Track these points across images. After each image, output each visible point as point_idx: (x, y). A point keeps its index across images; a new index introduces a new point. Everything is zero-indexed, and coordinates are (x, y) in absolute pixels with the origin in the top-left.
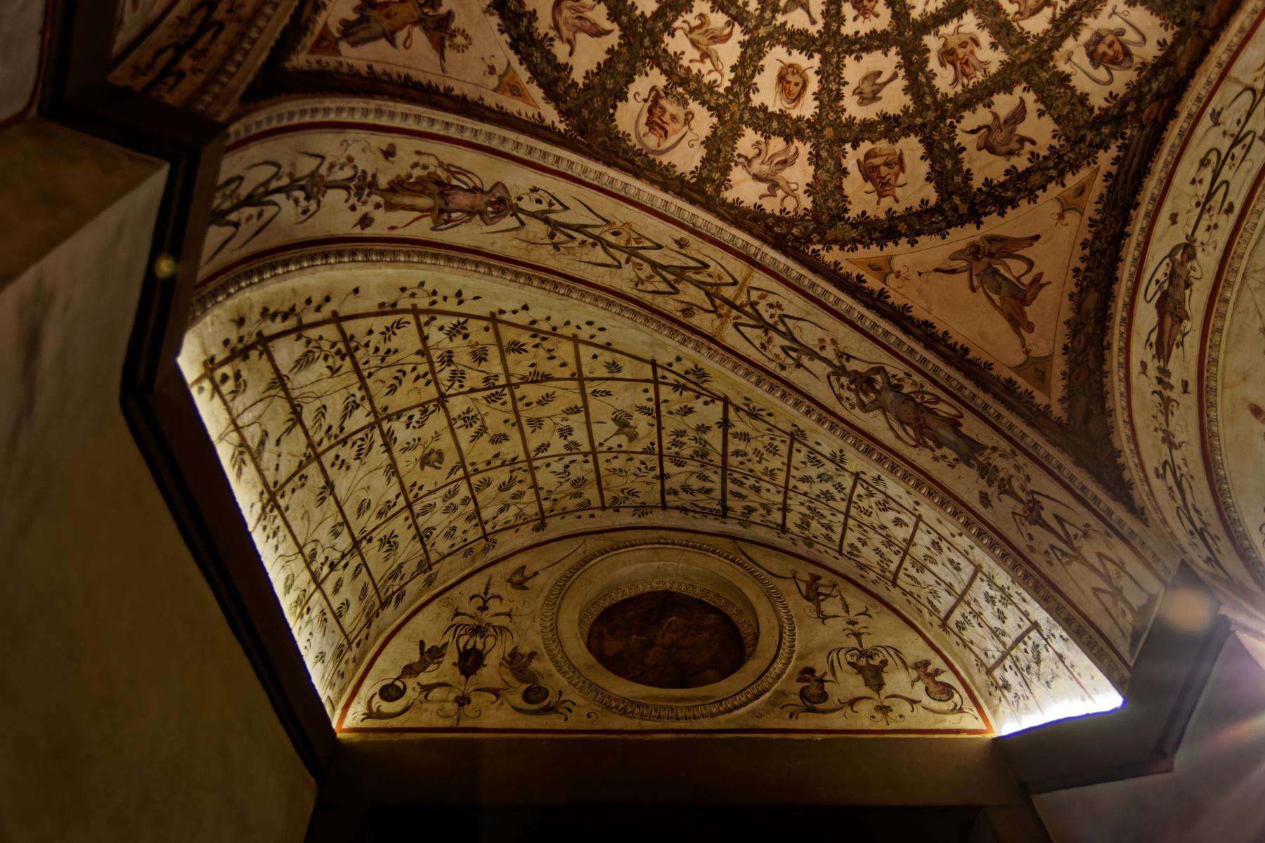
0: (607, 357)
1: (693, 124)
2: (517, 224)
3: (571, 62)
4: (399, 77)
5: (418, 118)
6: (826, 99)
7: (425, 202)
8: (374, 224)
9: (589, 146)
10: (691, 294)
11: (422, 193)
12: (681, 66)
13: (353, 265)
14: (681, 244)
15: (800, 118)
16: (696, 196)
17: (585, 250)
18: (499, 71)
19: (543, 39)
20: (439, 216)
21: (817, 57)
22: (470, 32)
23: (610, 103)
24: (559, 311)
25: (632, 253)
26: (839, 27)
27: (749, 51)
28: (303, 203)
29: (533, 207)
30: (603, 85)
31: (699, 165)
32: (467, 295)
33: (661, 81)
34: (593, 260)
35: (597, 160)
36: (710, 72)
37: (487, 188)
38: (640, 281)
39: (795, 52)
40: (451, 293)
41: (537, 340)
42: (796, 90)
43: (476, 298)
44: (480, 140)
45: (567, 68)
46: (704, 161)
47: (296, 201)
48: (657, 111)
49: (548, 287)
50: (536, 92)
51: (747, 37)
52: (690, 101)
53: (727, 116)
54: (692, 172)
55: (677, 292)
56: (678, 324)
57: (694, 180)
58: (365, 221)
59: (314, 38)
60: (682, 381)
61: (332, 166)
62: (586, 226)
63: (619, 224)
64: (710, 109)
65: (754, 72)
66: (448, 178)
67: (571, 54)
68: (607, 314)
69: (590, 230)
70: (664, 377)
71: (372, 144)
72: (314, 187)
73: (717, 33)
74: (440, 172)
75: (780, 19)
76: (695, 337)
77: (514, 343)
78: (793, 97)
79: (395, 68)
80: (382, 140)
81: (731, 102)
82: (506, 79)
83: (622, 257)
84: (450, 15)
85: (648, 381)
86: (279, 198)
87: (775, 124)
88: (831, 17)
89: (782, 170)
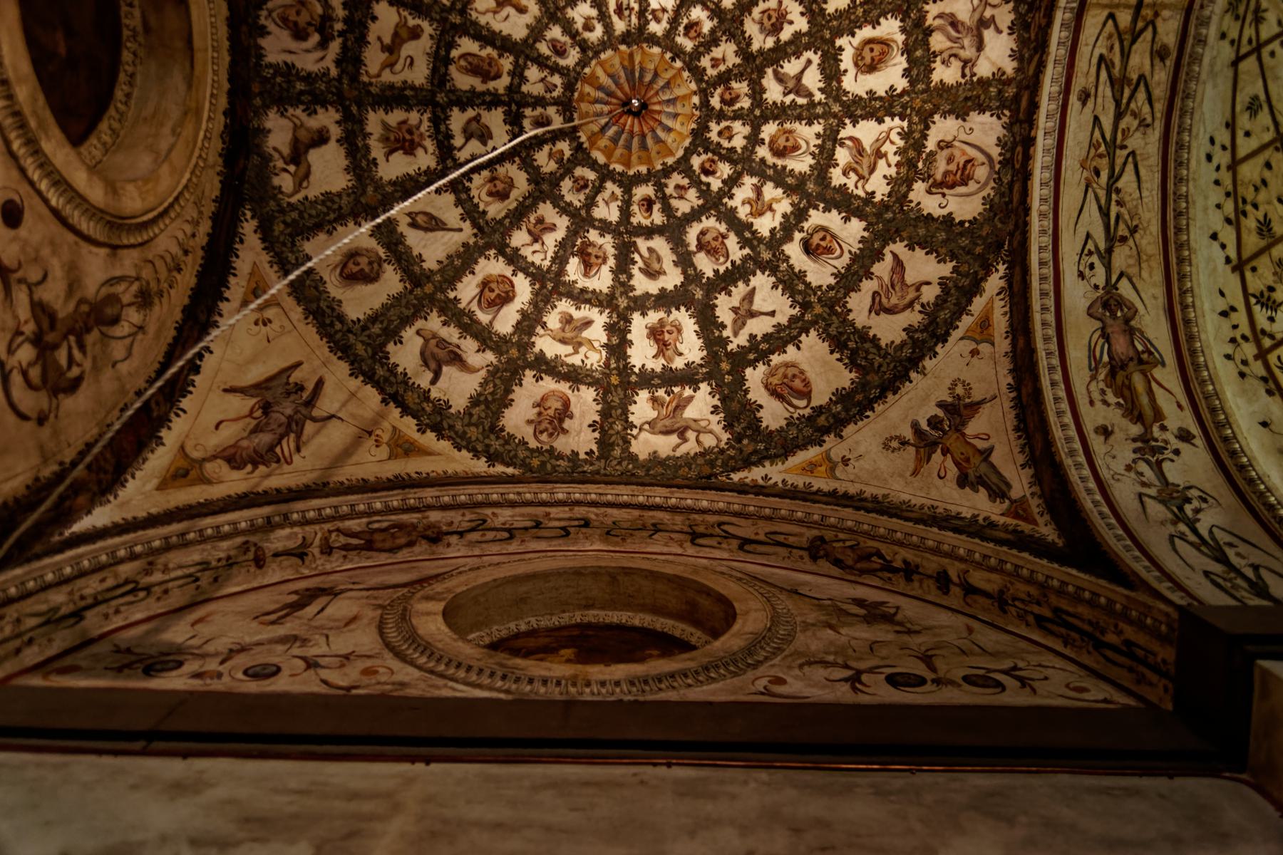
0: (1244, 121)
1: (949, 138)
2: (1124, 281)
3: (935, 280)
4: (1019, 437)
5: (1060, 414)
6: (875, 13)
7: (1138, 381)
8: (1184, 426)
9: (1011, 235)
10: (1140, 59)
11: (1130, 388)
12: (898, 173)
13: (1240, 437)
14: (1085, 97)
15: (903, 30)
16: (1024, 103)
17: (1127, 198)
18: (973, 346)
19: (926, 314)
20: (1147, 363)
21: (839, 42)
22: (948, 383)
23: (958, 229)
24: (1206, 198)
25: (1112, 146)
26: (804, 35)
27: (859, 112)
28: (1196, 504)
29: (1100, 270)
30: (945, 242)
31: (988, 114)
32: (1222, 305)
33: (919, 186)
34: (1135, 185)
35: (1026, 224)
36: (892, 143)
37: (1098, 324)
38: (1144, 125)
39: (842, 67)
40: (1226, 324)
41: (1249, 208)
42: (877, 48)
43: (1222, 294)
44: (1054, 347)
45: (943, 282)
46: (982, 111)
47: (1197, 511)
48: (950, 179)
49: (1184, 222)
50: (978, 304)
51: (847, 121)
52: (928, 150)
53: (928, 106)
54: (999, 118)
55: (1142, 77)
56: (1181, 59)
57: (1007, 112)
58: (1185, 436)
59: (1020, 523)
60: (1250, 17)
61: (1144, 484)
62: (1100, 208)
63: (1085, 174)
64: (927, 127)
65: (876, 99)
66: (1104, 367)
67: (928, 283)
68: (1194, 144)
69: (1103, 202)
70: (1250, 41)
71: (1104, 451)
72: (1175, 498)
73: (854, 151)
74: (1102, 377)
75: (819, 96)
76: (1192, 31)
77: (1260, 233)
78: (885, 48)
79: (1014, 444)
80: (1096, 442)
81: (913, 109)
82: (977, 337)
83: (1121, 155)
84: (941, 405)
85: (1259, 59)
86: (1203, 528)
87: (919, 53)
88: (798, 47)
89: (963, 24)
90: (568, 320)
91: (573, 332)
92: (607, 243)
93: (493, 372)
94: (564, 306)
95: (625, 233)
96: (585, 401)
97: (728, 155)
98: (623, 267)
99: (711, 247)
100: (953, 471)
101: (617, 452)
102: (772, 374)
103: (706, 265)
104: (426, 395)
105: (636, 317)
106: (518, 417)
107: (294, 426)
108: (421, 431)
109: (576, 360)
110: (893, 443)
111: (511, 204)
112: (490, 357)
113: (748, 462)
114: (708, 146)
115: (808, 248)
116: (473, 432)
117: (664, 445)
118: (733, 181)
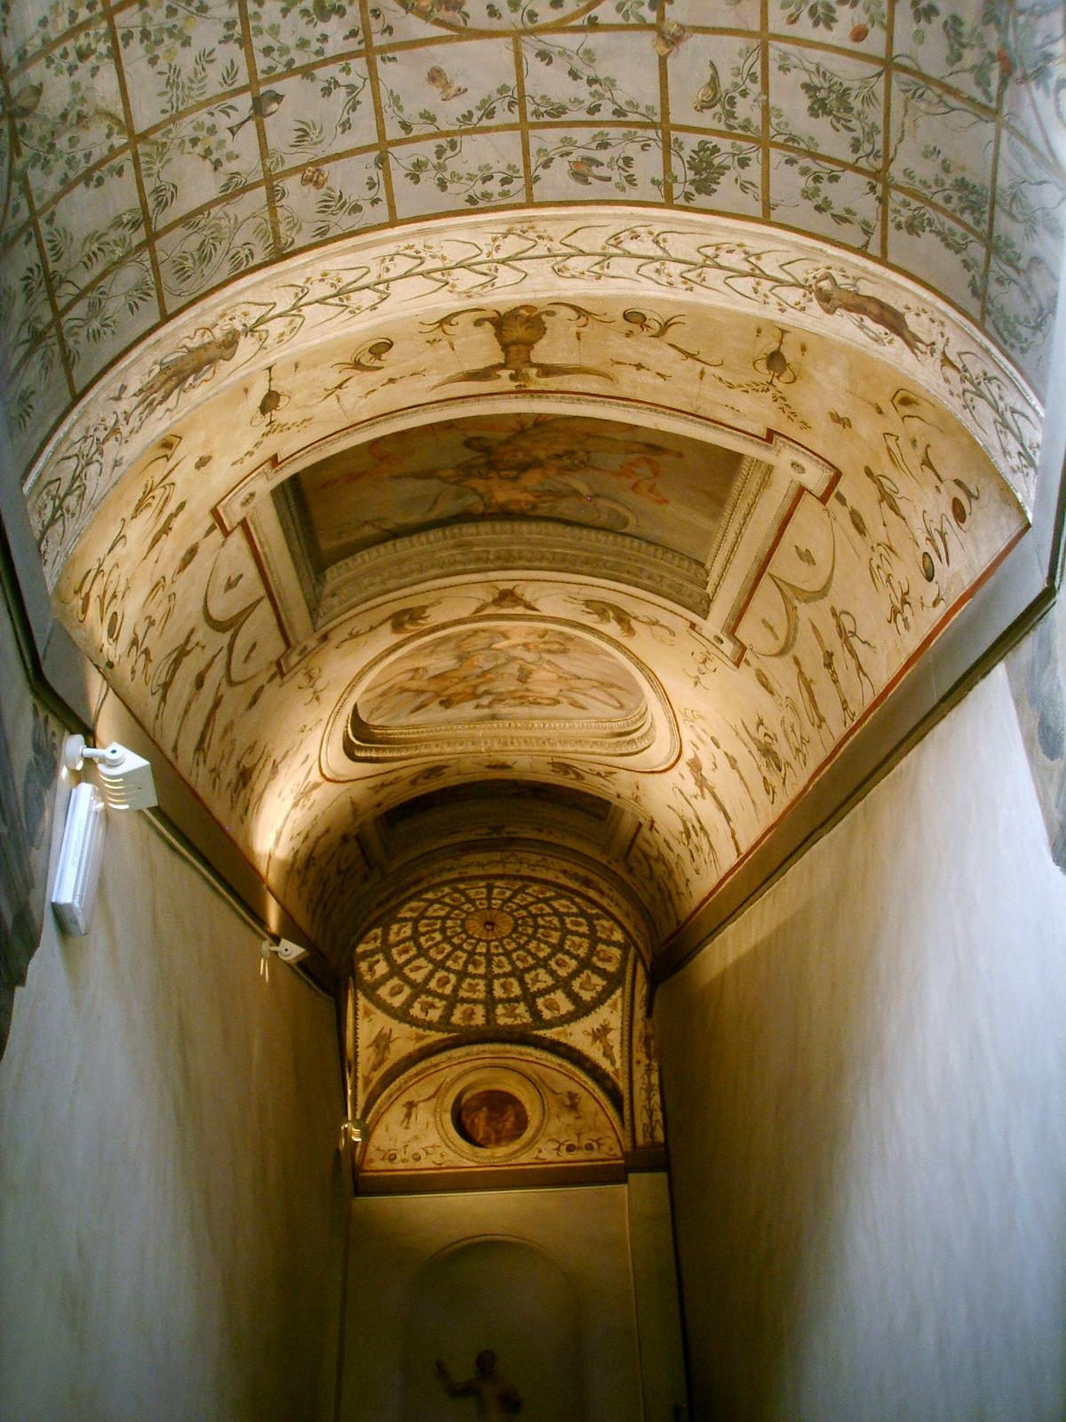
50: (614, 997)
90: (470, 985)
91: (472, 988)
92: (482, 959)
93: (446, 1007)
94: (468, 980)
95: (489, 957)
96: (480, 1010)
97: (527, 935)
99: (523, 960)
100: (602, 1050)
101: (492, 1022)
102: (546, 1000)
103: (520, 965)
104: (424, 1020)
105: (495, 981)
106: (457, 1018)
107: (387, 1047)
108: (424, 1030)
109: (475, 997)
112: (444, 1003)
113: (538, 1029)
114: (518, 932)
115: (557, 963)
116: (442, 1027)
117: (509, 1021)
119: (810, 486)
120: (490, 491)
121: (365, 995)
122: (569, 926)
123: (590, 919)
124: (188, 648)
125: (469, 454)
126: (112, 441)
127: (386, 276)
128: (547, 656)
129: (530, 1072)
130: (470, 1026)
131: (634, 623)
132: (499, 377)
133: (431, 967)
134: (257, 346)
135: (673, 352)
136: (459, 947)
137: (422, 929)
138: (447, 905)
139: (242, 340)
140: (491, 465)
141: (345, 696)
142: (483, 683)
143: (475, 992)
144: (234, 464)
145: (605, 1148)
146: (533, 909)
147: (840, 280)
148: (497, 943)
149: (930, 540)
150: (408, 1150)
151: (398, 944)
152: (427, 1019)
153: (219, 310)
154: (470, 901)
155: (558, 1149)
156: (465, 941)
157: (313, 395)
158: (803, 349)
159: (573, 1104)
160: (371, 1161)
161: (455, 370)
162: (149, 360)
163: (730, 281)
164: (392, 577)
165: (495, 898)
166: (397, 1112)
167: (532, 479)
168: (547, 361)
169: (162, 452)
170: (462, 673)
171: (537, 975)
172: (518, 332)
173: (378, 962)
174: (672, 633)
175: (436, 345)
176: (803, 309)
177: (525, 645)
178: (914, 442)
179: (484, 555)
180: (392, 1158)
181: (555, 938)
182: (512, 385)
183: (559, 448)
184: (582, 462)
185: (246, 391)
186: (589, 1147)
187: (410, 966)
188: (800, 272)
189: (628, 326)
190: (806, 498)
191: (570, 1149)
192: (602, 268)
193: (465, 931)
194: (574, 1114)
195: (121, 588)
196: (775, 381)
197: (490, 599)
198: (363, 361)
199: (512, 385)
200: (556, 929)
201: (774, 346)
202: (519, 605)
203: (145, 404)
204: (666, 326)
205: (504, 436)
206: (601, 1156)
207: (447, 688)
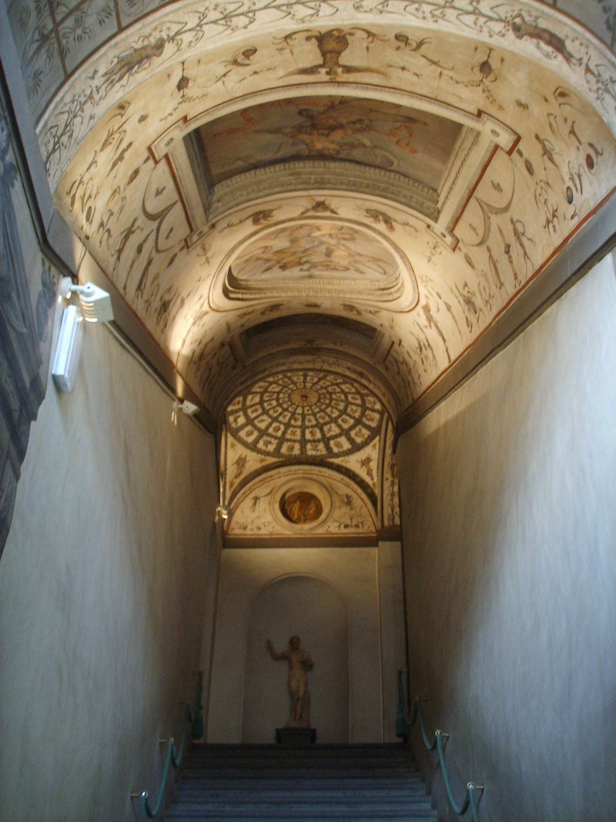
91: (293, 433)
92: (300, 417)
93: (278, 444)
94: (291, 429)
95: (303, 416)
96: (297, 446)
98: (303, 420)
99: (323, 418)
103: (321, 421)
106: (284, 450)
107: (243, 465)
110: (357, 461)
111: (278, 413)
113: (331, 457)
115: (342, 421)
117: (314, 453)
118: (327, 408)
119: (502, 145)
120: (312, 142)
121: (232, 435)
122: (350, 400)
123: (362, 396)
124: (134, 229)
125: (299, 120)
126: (89, 104)
127: (253, 8)
128: (342, 242)
129: (325, 482)
130: (291, 455)
131: (394, 224)
132: (319, 72)
133: (270, 420)
134: (176, 49)
135: (424, 61)
136: (287, 410)
137: (266, 398)
138: (280, 385)
139: (167, 45)
140: (313, 126)
141: (224, 261)
142: (305, 256)
143: (294, 435)
144: (161, 120)
145: (366, 527)
146: (330, 389)
147: (527, 18)
148: (308, 408)
149: (572, 179)
150: (254, 524)
151: (251, 406)
152: (267, 450)
153: (153, 25)
154: (295, 383)
155: (339, 526)
156: (290, 406)
157: (209, 80)
158: (502, 60)
159: (348, 501)
160: (233, 529)
161: (293, 67)
162: (111, 55)
163: (460, 17)
164: (253, 191)
165: (308, 382)
166: (248, 502)
167: (337, 136)
168: (348, 64)
169: (119, 111)
170: (293, 250)
171: (331, 427)
172: (331, 45)
173: (239, 416)
174: (416, 230)
175: (283, 52)
176: (504, 35)
177: (330, 235)
178: (566, 120)
179: (308, 180)
180: (245, 528)
181: (341, 406)
182: (327, 78)
183: (354, 117)
184: (367, 126)
185: (169, 76)
186: (357, 526)
187: (258, 420)
188: (503, 12)
189: (398, 44)
190: (499, 152)
191: (346, 526)
192: (383, 6)
193: (290, 400)
194: (349, 507)
195: (94, 192)
196: (484, 80)
197: (310, 207)
198: (239, 60)
199: (327, 78)
200: (342, 401)
201: (485, 58)
202: (327, 210)
203: (109, 82)
204: (420, 44)
205: (322, 109)
206: (363, 531)
207: (283, 258)
